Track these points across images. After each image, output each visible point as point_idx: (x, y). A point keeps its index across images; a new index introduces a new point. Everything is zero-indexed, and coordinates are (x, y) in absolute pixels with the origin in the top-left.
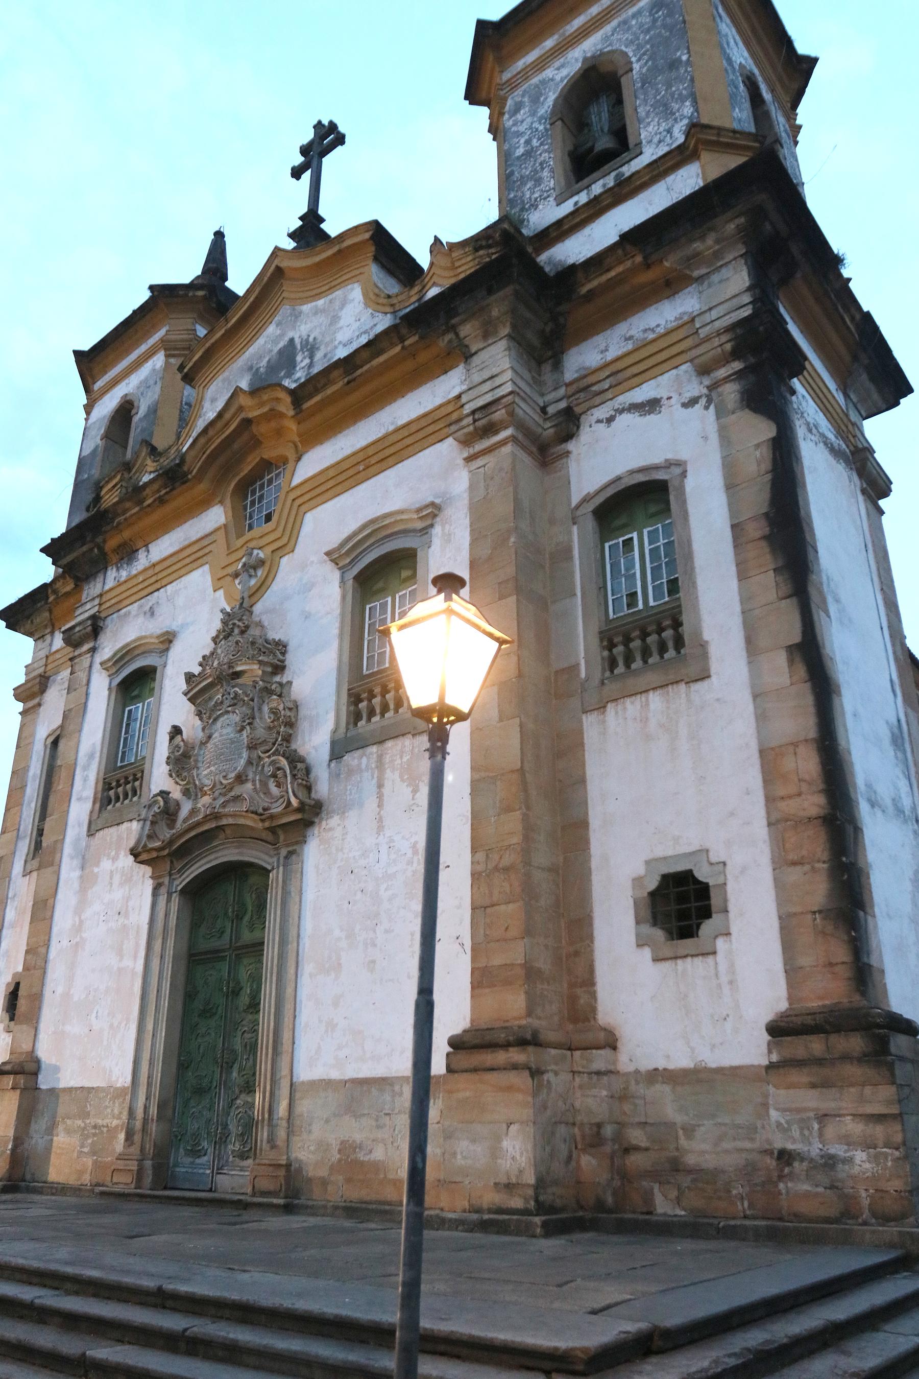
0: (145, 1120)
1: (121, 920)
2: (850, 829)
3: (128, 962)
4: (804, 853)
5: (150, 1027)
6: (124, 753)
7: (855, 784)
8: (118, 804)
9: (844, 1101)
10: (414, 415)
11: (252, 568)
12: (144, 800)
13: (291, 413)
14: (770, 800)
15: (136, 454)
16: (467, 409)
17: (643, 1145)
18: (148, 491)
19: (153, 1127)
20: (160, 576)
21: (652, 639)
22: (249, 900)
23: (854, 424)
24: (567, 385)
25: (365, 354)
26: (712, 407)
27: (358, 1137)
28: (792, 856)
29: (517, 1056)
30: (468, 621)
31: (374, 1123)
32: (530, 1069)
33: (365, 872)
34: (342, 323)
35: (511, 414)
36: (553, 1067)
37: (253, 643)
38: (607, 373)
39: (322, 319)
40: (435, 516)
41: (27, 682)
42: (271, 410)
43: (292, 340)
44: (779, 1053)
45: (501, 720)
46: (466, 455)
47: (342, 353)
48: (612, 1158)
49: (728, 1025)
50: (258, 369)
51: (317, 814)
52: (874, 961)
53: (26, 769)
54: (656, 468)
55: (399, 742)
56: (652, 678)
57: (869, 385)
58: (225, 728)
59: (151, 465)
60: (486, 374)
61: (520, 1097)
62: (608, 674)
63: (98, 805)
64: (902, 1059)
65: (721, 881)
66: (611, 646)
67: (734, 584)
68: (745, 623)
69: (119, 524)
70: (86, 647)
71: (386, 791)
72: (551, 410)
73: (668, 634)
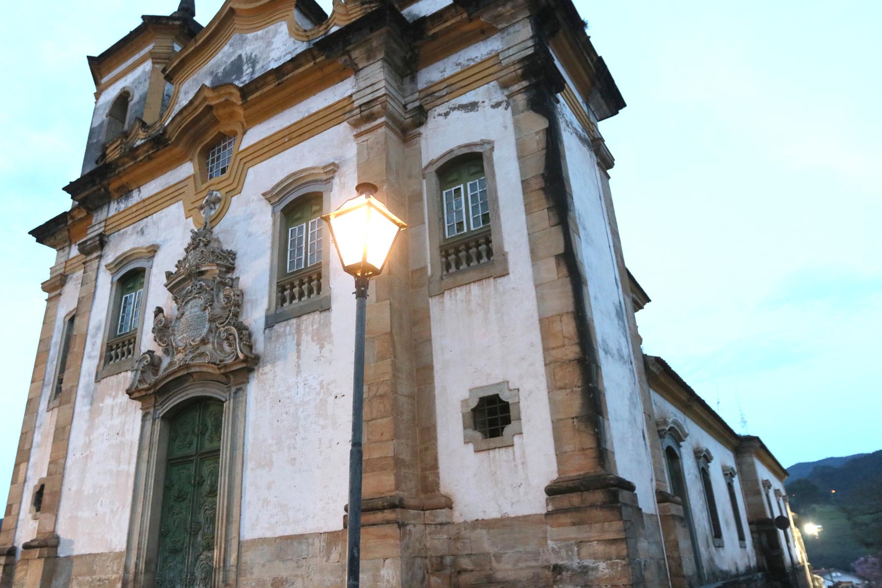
1: (119, 438)
2: (593, 366)
3: (124, 467)
4: (567, 381)
5: (139, 510)
6: (122, 326)
7: (596, 340)
8: (118, 360)
9: (593, 532)
10: (321, 107)
12: (136, 357)
13: (240, 103)
14: (546, 350)
15: (132, 127)
16: (356, 104)
17: (470, 568)
18: (140, 151)
19: (142, 578)
20: (148, 208)
21: (473, 251)
22: (210, 422)
23: (592, 124)
24: (420, 92)
25: (290, 67)
26: (510, 108)
27: (284, 575)
28: (559, 384)
29: (389, 515)
30: (381, 211)
31: (296, 565)
32: (398, 523)
33: (289, 401)
34: (274, 46)
35: (385, 108)
36: (413, 522)
37: (213, 252)
38: (445, 85)
39: (260, 43)
40: (335, 171)
41: (51, 279)
42: (226, 100)
43: (240, 56)
44: (553, 505)
45: (377, 301)
46: (355, 133)
47: (274, 65)
48: (450, 578)
49: (522, 490)
50: (217, 74)
51: (256, 364)
52: (608, 446)
53: (50, 338)
54: (475, 145)
56: (473, 275)
57: (602, 101)
58: (193, 309)
59: (142, 134)
60: (369, 83)
61: (392, 541)
62: (445, 273)
63: (103, 361)
64: (625, 505)
65: (516, 401)
66: (447, 255)
67: (523, 217)
68: (530, 240)
69: (119, 172)
70: (95, 255)
71: (302, 348)
72: (410, 107)
73: (483, 247)
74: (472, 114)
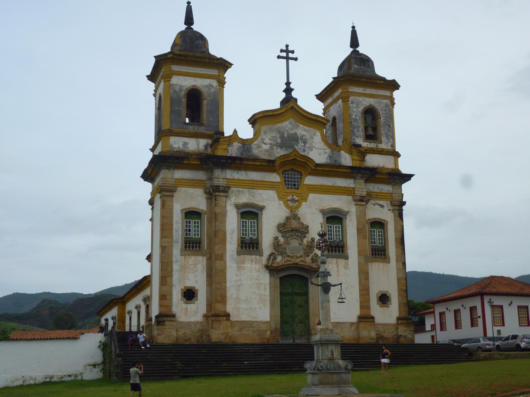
0: (276, 328)
11: (293, 200)
14: (398, 286)
20: (255, 185)
29: (372, 320)
34: (314, 140)
55: (342, 260)
63: (240, 247)
66: (372, 251)
74: (382, 209)
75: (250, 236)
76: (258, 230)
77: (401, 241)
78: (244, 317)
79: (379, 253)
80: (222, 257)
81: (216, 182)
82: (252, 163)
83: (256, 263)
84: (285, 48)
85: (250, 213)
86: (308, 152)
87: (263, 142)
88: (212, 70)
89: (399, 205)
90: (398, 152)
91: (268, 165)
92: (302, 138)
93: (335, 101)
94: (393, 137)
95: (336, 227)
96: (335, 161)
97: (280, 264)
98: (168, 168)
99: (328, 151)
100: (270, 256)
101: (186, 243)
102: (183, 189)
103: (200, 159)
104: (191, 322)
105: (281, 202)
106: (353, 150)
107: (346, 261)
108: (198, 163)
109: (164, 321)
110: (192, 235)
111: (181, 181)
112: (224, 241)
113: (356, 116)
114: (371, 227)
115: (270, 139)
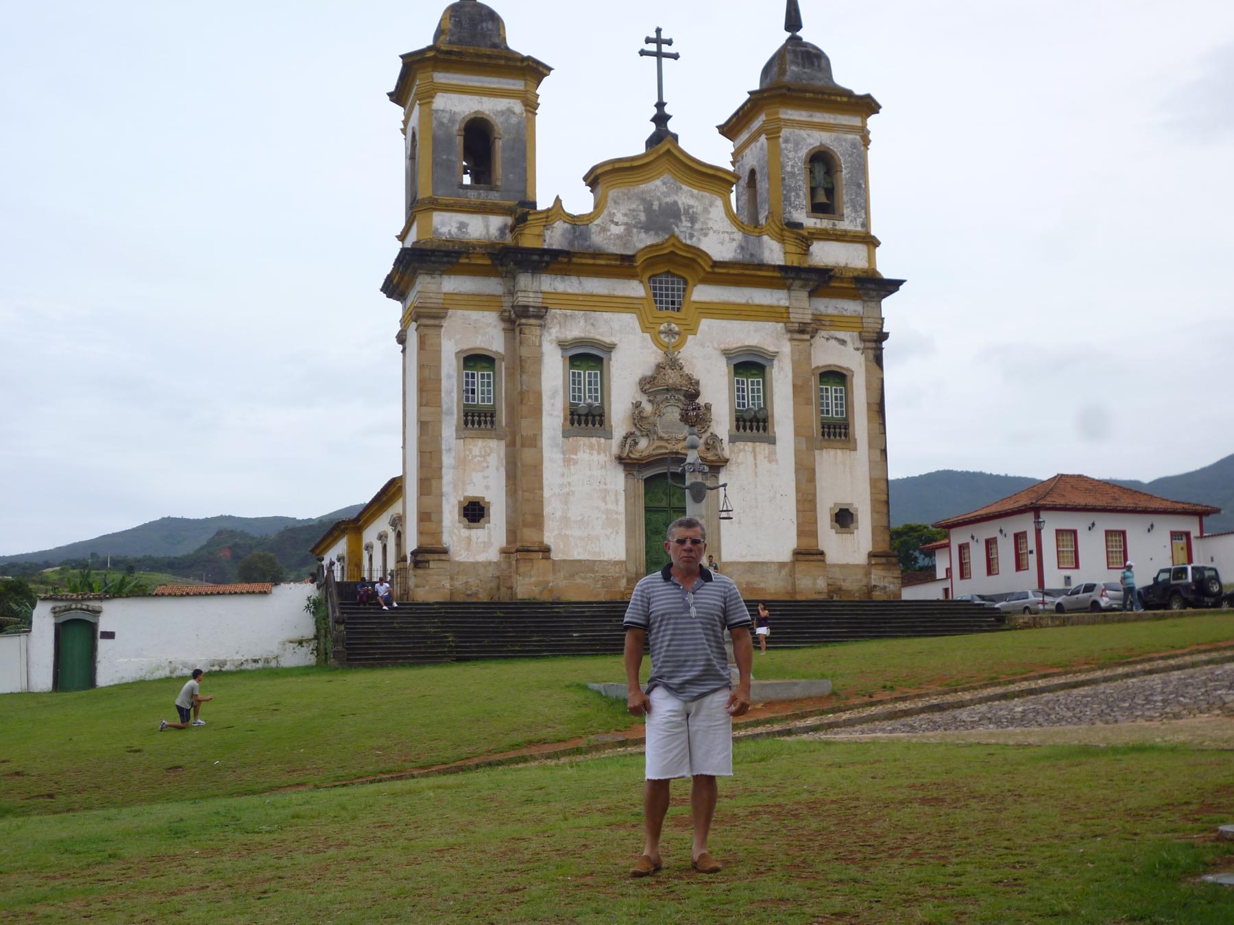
3: (611, 506)
11: (670, 333)
27: (754, 580)
29: (819, 557)
75: (586, 401)
76: (603, 388)
77: (878, 409)
78: (578, 554)
79: (836, 431)
80: (534, 441)
81: (522, 299)
82: (591, 261)
83: (599, 453)
84: (654, 36)
85: (588, 358)
86: (699, 240)
87: (612, 221)
88: (512, 81)
89: (875, 341)
90: (874, 237)
91: (622, 266)
92: (687, 212)
93: (753, 138)
94: (866, 208)
95: (753, 383)
96: (752, 255)
97: (645, 454)
98: (431, 272)
99: (738, 236)
100: (626, 438)
101: (466, 415)
102: (460, 312)
103: (491, 255)
104: (478, 563)
105: (647, 336)
106: (786, 233)
107: (772, 446)
108: (488, 262)
109: (428, 561)
110: (478, 399)
111: (459, 298)
112: (537, 411)
113: (793, 166)
114: (822, 382)
115: (625, 215)
